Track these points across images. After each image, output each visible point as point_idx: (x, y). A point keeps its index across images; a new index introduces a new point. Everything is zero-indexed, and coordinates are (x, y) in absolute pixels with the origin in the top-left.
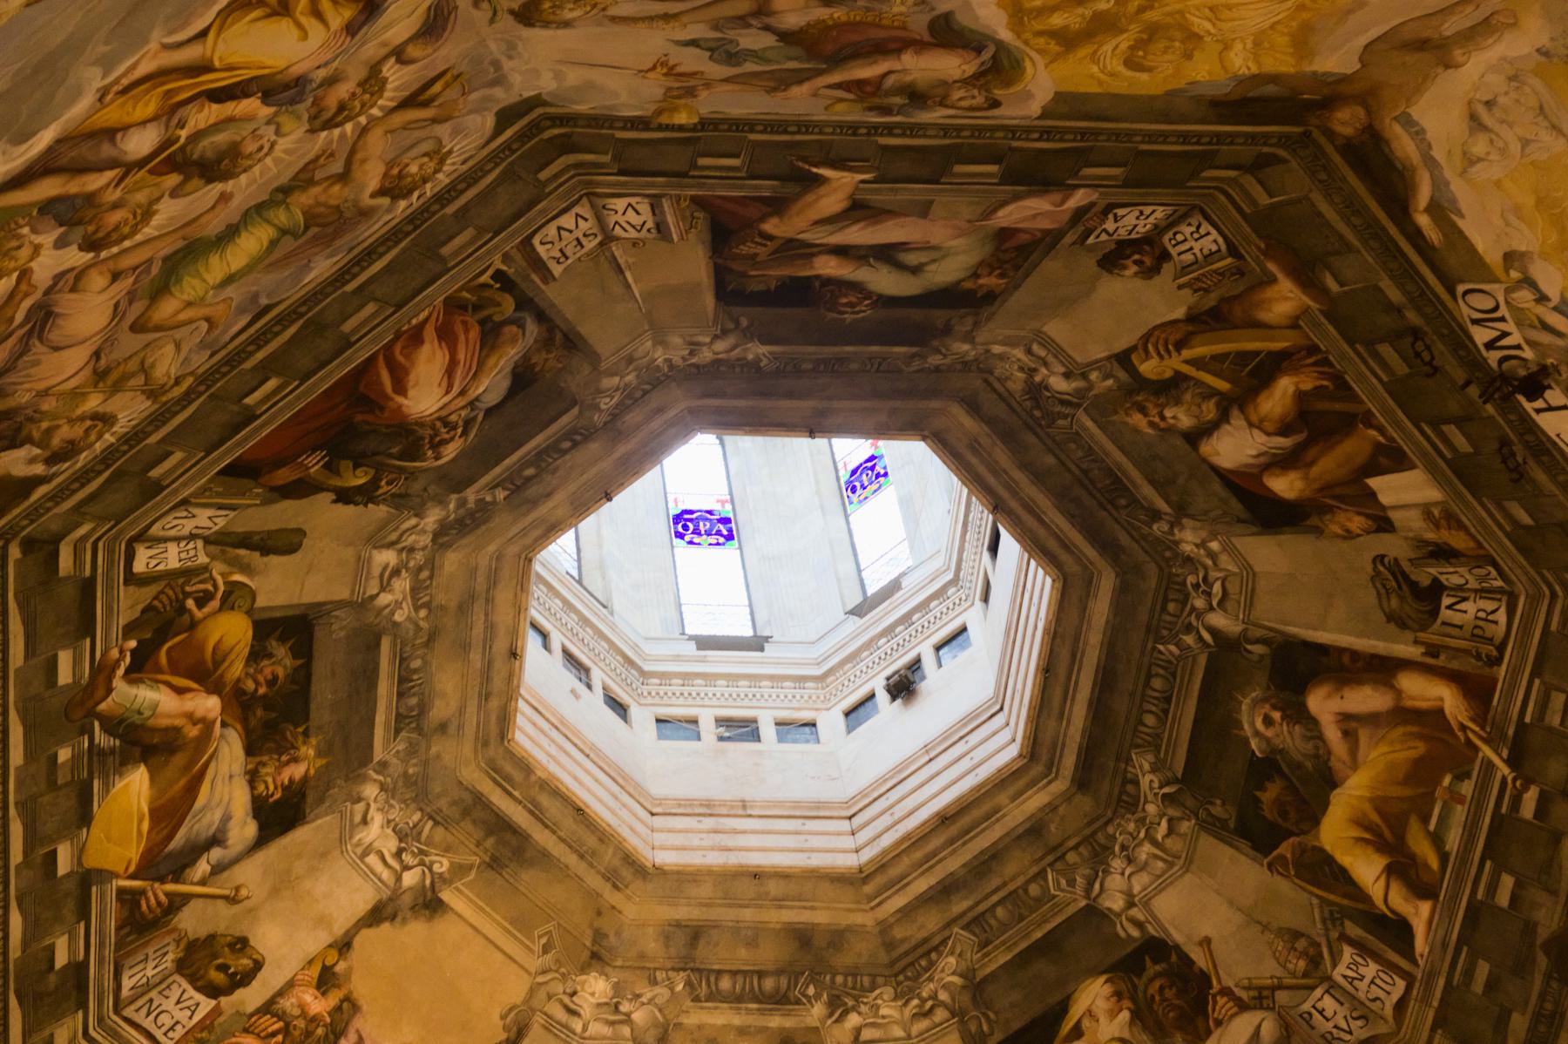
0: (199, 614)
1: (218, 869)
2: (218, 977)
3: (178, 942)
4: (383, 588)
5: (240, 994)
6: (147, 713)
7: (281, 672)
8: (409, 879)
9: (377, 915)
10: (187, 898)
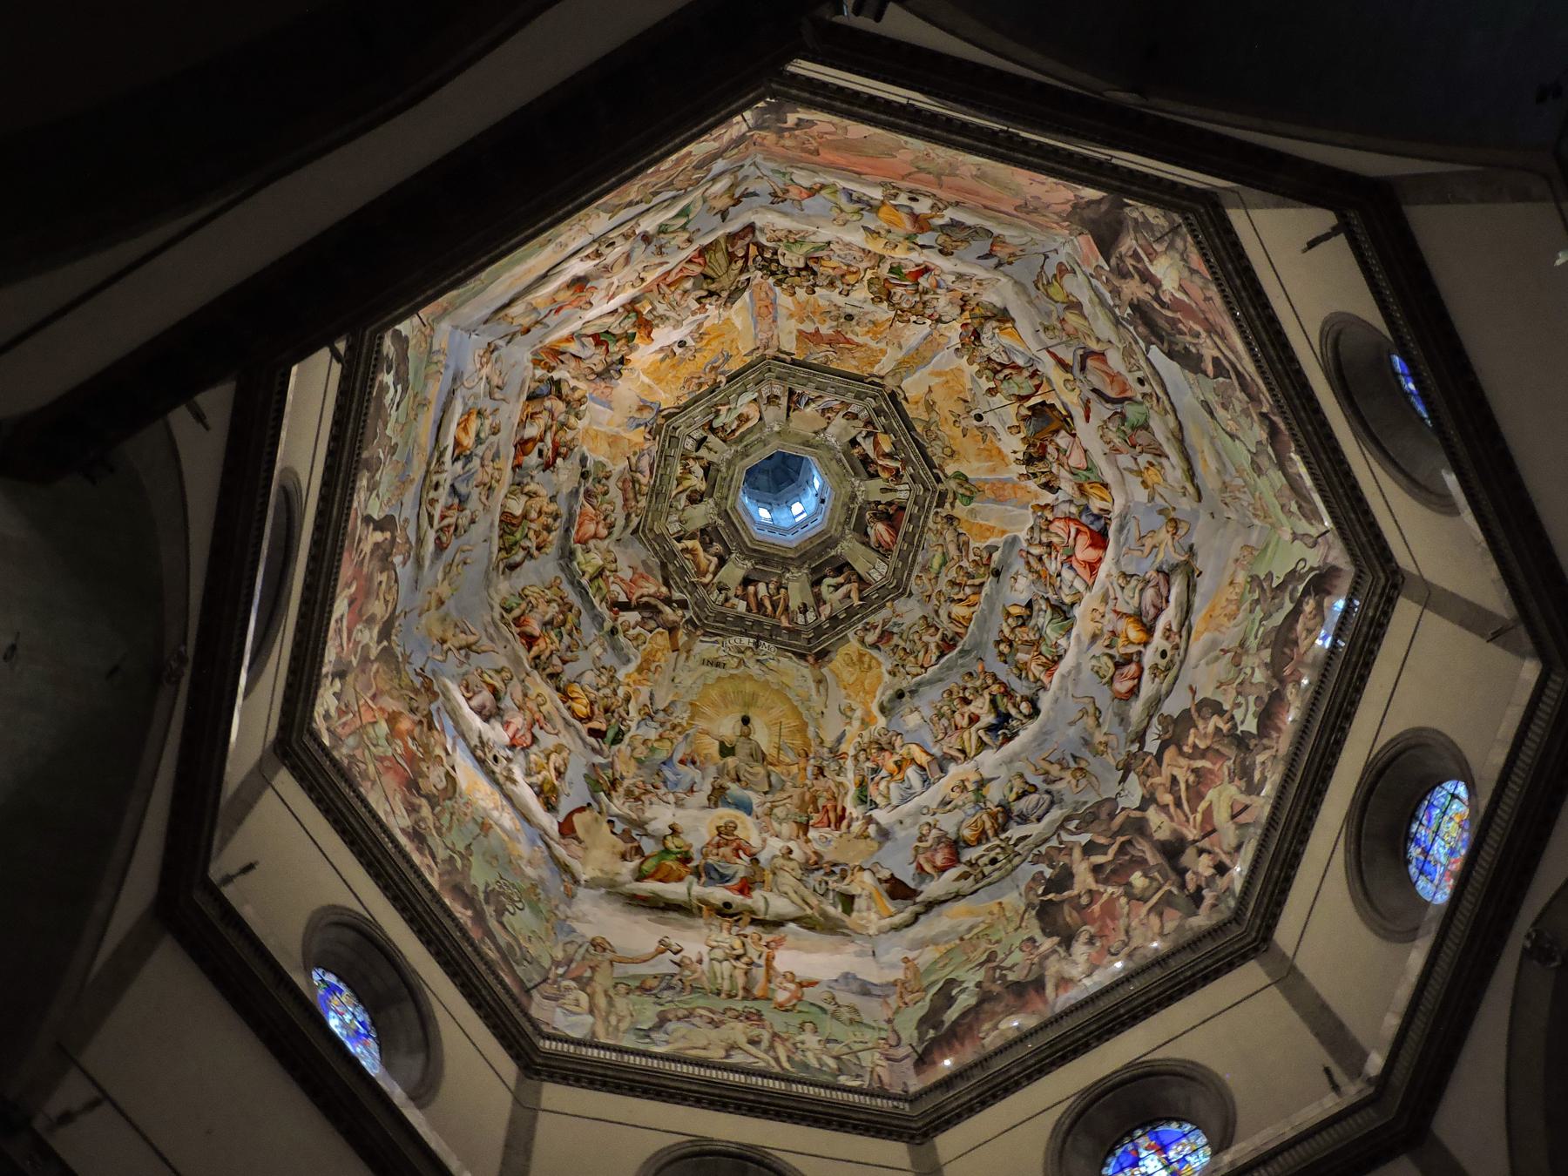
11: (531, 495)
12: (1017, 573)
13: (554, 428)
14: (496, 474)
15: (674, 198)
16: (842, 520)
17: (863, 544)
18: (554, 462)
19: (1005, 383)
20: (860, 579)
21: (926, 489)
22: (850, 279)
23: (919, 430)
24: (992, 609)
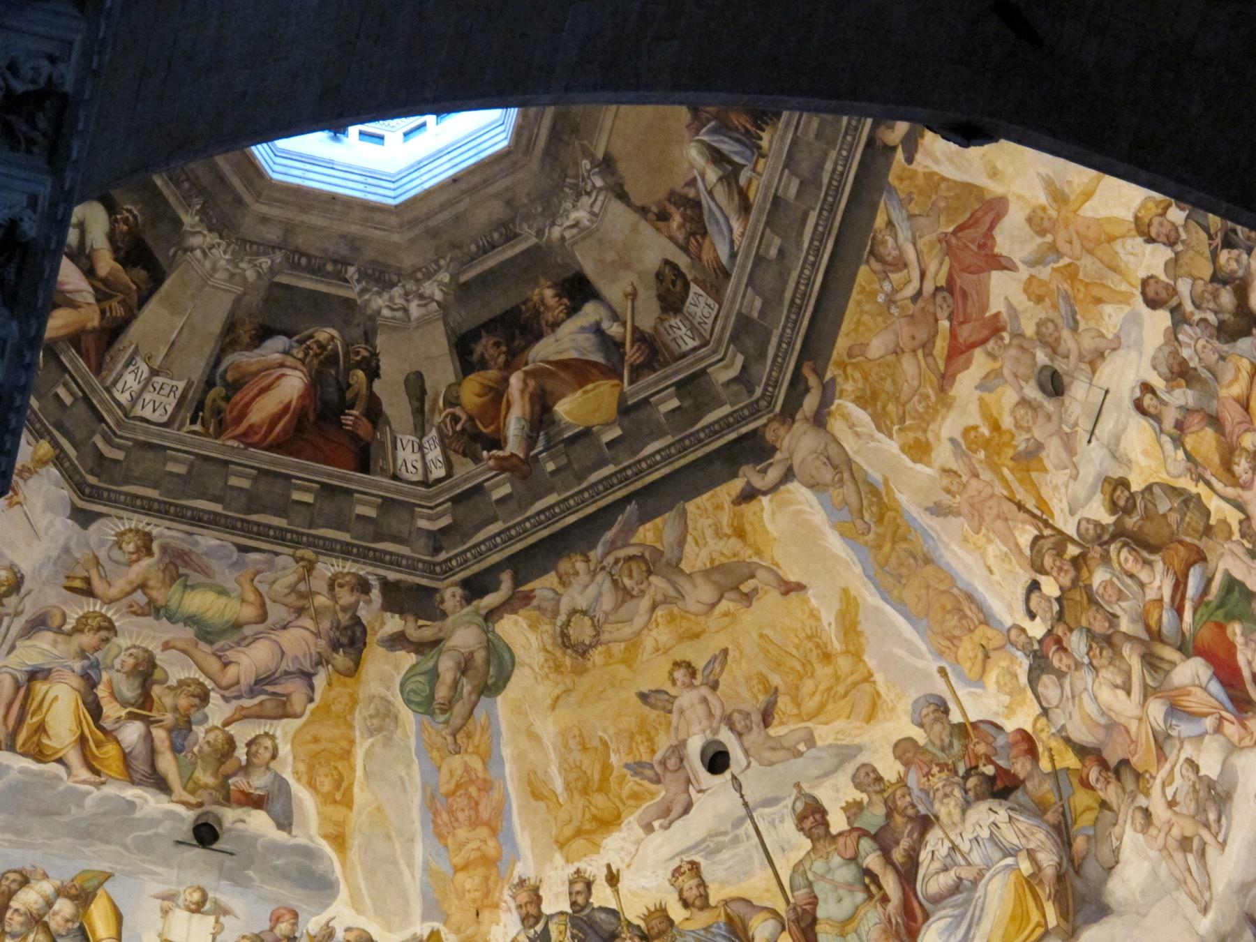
0: (464, 417)
1: (615, 317)
2: (679, 284)
3: (662, 321)
4: (433, 300)
5: (684, 269)
6: (523, 422)
7: (492, 341)
8: (599, 183)
9: (622, 196)
10: (635, 329)
12: (221, 911)
16: (300, 241)
17: (230, 327)
19: (846, 874)
20: (112, 332)
21: (437, 540)
22: (1204, 441)
23: (646, 534)
24: (88, 832)
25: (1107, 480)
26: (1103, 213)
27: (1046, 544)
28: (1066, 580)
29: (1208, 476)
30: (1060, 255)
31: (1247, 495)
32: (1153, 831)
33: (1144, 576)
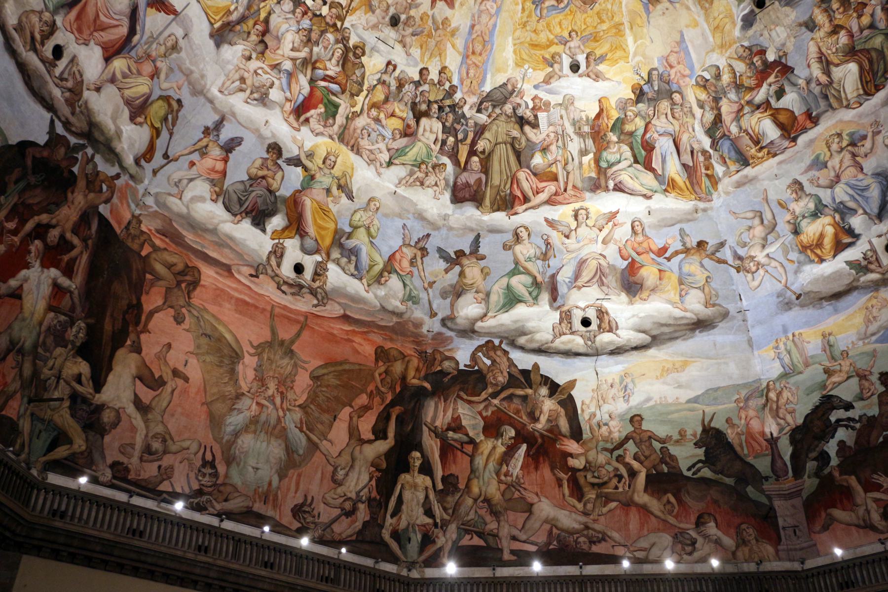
11: (826, 65)
13: (747, 98)
14: (835, 147)
15: (513, 344)
18: (776, 63)
22: (379, 95)
25: (364, 45)
26: (448, 52)
27: (340, 10)
28: (328, 19)
29: (370, 96)
30: (436, 30)
31: (365, 115)
32: (244, 61)
33: (334, 61)
